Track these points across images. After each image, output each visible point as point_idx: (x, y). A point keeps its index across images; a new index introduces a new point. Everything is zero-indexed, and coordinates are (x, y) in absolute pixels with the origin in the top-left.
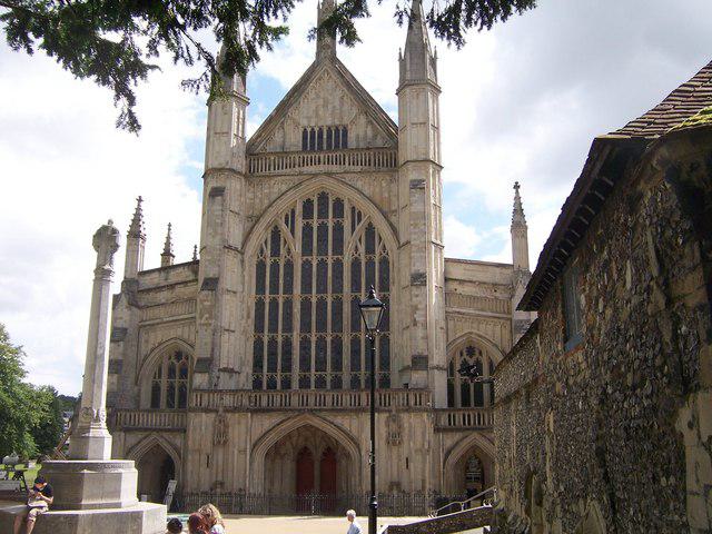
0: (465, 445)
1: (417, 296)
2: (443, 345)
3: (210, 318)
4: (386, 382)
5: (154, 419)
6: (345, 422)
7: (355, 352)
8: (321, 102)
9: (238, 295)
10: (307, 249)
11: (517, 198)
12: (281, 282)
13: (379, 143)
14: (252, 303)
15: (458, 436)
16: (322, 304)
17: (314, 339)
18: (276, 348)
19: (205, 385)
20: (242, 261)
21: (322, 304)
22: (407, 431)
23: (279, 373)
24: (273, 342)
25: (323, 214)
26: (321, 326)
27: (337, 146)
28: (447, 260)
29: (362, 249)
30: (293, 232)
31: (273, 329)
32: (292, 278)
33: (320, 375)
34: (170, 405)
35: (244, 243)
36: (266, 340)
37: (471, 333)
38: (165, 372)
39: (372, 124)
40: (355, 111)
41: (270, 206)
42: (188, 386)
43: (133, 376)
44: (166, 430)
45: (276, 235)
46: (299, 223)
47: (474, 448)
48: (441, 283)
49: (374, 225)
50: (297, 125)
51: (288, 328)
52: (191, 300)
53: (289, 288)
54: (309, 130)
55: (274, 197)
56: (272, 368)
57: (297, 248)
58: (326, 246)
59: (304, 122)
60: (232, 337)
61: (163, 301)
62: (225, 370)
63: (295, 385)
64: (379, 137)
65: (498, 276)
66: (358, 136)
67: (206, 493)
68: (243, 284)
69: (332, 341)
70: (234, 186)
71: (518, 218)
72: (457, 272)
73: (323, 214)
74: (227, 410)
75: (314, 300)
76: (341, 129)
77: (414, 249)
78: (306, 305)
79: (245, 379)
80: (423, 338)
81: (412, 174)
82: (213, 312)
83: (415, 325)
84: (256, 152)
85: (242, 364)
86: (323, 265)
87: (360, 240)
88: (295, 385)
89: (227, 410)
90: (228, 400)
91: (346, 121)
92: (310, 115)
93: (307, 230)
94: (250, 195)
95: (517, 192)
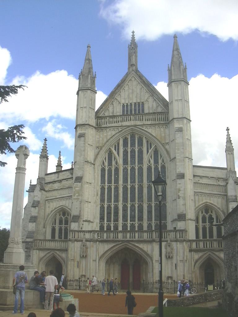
1: (180, 184)
2: (193, 208)
3: (79, 196)
5: (52, 245)
6: (146, 247)
8: (130, 91)
9: (92, 184)
10: (125, 162)
11: (228, 135)
13: (159, 110)
14: (99, 188)
15: (201, 254)
16: (133, 188)
17: (129, 206)
18: (111, 210)
19: (76, 229)
20: (94, 168)
21: (133, 188)
22: (175, 251)
23: (112, 222)
24: (109, 207)
25: (133, 145)
27: (139, 112)
28: (194, 166)
29: (152, 161)
30: (118, 153)
31: (109, 200)
32: (118, 176)
33: (133, 223)
34: (60, 237)
35: (95, 160)
36: (106, 206)
37: (207, 202)
38: (57, 221)
39: (156, 101)
40: (147, 95)
42: (68, 228)
43: (42, 223)
44: (58, 250)
45: (110, 154)
48: (192, 177)
49: (158, 150)
52: (70, 187)
53: (117, 181)
54: (125, 104)
55: (108, 138)
56: (109, 220)
57: (121, 161)
58: (135, 160)
59: (123, 101)
60: (90, 205)
61: (57, 188)
62: (86, 221)
63: (120, 228)
64: (159, 107)
65: (221, 174)
66: (149, 107)
67: (77, 280)
68: (95, 179)
69: (138, 207)
70: (91, 133)
71: (229, 145)
72: (199, 172)
73: (133, 145)
74: (87, 241)
75: (129, 187)
76: (141, 103)
77: (177, 161)
78: (125, 189)
79: (96, 226)
80: (183, 205)
81: (177, 125)
82: (80, 193)
83: (179, 198)
84: (100, 116)
85: (94, 218)
86: (133, 169)
87: (151, 157)
88: (120, 228)
89: (87, 241)
90: (88, 236)
92: (125, 97)
93: (125, 153)
94: (98, 137)
95: (228, 132)
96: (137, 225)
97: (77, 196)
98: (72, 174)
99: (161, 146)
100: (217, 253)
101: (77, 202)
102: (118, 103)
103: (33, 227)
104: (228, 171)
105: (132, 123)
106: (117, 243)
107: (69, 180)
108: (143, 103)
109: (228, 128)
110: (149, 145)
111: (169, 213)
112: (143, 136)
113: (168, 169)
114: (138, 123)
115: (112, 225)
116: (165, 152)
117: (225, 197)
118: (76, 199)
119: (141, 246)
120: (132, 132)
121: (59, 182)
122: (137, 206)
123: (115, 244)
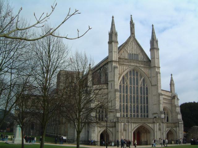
0: (169, 130)
4: (147, 116)
7: (141, 109)
8: (132, 47)
12: (125, 90)
13: (145, 60)
17: (133, 105)
18: (124, 107)
24: (124, 105)
26: (134, 102)
28: (162, 90)
29: (142, 85)
31: (124, 102)
32: (127, 90)
36: (122, 105)
41: (124, 71)
45: (123, 78)
46: (129, 77)
47: (170, 130)
50: (127, 52)
51: (127, 102)
53: (127, 92)
57: (129, 83)
63: (129, 116)
72: (163, 93)
73: (134, 75)
86: (134, 87)
91: (137, 53)
93: (131, 78)
96: (136, 115)
98: (107, 86)
99: (147, 77)
100: (173, 128)
102: (126, 52)
105: (135, 64)
110: (141, 77)
111: (151, 110)
114: (138, 65)
115: (125, 115)
116: (149, 82)
118: (117, 101)
119: (150, 125)
122: (136, 105)
123: (138, 124)
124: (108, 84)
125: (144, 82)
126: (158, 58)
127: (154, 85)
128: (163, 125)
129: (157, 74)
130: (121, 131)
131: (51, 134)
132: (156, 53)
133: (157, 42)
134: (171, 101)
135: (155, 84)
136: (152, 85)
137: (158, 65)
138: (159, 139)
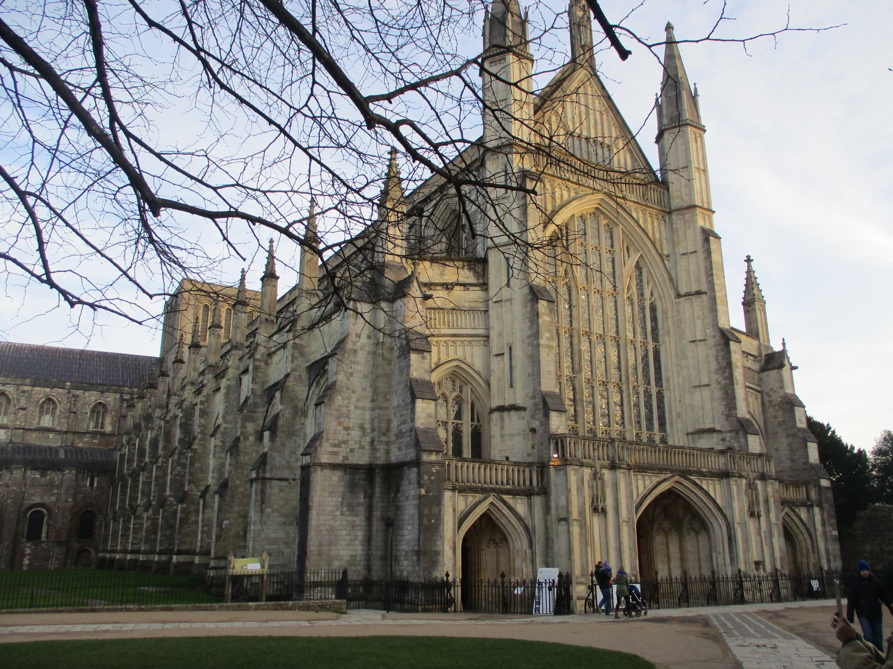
11: (750, 272)
29: (634, 289)
83: (737, 384)
97: (548, 339)
101: (548, 355)
103: (430, 416)
104: (760, 344)
106: (662, 477)
107: (471, 288)
108: (608, 146)
109: (748, 257)
112: (617, 225)
113: (665, 313)
117: (759, 395)
120: (597, 208)
121: (447, 289)
123: (658, 479)
124: (484, 261)
125: (641, 281)
126: (705, 171)
127: (688, 294)
128: (765, 490)
129: (707, 240)
130: (582, 513)
131: (129, 557)
132: (693, 146)
133: (694, 98)
134: (761, 380)
135: (694, 288)
136: (682, 292)
137: (705, 200)
138: (757, 563)
